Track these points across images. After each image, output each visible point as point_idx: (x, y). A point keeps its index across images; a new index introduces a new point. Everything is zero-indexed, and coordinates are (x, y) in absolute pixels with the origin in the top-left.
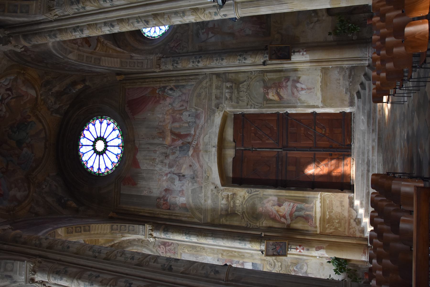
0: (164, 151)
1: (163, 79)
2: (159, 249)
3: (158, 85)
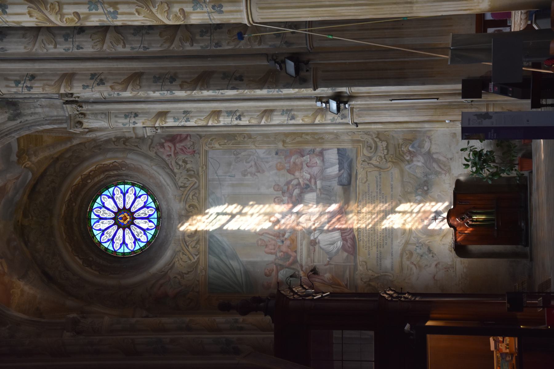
2: (162, 150)
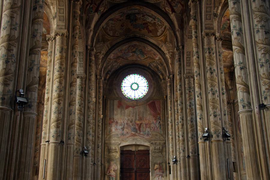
0: (133, 120)
1: (164, 118)
3: (161, 116)
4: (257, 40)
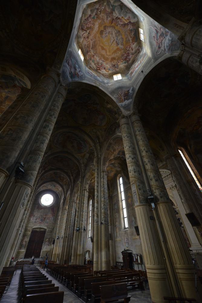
4: (102, 200)
